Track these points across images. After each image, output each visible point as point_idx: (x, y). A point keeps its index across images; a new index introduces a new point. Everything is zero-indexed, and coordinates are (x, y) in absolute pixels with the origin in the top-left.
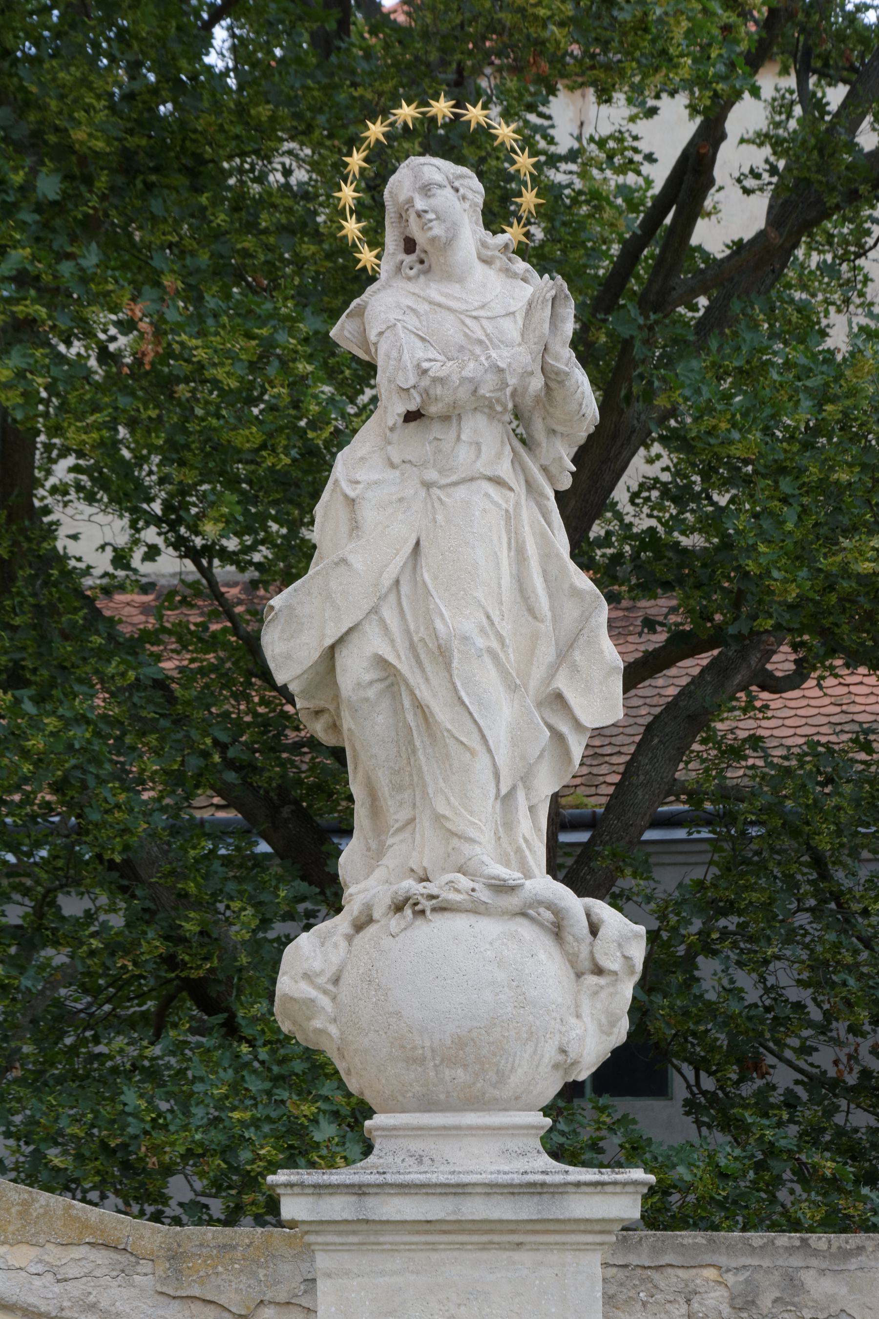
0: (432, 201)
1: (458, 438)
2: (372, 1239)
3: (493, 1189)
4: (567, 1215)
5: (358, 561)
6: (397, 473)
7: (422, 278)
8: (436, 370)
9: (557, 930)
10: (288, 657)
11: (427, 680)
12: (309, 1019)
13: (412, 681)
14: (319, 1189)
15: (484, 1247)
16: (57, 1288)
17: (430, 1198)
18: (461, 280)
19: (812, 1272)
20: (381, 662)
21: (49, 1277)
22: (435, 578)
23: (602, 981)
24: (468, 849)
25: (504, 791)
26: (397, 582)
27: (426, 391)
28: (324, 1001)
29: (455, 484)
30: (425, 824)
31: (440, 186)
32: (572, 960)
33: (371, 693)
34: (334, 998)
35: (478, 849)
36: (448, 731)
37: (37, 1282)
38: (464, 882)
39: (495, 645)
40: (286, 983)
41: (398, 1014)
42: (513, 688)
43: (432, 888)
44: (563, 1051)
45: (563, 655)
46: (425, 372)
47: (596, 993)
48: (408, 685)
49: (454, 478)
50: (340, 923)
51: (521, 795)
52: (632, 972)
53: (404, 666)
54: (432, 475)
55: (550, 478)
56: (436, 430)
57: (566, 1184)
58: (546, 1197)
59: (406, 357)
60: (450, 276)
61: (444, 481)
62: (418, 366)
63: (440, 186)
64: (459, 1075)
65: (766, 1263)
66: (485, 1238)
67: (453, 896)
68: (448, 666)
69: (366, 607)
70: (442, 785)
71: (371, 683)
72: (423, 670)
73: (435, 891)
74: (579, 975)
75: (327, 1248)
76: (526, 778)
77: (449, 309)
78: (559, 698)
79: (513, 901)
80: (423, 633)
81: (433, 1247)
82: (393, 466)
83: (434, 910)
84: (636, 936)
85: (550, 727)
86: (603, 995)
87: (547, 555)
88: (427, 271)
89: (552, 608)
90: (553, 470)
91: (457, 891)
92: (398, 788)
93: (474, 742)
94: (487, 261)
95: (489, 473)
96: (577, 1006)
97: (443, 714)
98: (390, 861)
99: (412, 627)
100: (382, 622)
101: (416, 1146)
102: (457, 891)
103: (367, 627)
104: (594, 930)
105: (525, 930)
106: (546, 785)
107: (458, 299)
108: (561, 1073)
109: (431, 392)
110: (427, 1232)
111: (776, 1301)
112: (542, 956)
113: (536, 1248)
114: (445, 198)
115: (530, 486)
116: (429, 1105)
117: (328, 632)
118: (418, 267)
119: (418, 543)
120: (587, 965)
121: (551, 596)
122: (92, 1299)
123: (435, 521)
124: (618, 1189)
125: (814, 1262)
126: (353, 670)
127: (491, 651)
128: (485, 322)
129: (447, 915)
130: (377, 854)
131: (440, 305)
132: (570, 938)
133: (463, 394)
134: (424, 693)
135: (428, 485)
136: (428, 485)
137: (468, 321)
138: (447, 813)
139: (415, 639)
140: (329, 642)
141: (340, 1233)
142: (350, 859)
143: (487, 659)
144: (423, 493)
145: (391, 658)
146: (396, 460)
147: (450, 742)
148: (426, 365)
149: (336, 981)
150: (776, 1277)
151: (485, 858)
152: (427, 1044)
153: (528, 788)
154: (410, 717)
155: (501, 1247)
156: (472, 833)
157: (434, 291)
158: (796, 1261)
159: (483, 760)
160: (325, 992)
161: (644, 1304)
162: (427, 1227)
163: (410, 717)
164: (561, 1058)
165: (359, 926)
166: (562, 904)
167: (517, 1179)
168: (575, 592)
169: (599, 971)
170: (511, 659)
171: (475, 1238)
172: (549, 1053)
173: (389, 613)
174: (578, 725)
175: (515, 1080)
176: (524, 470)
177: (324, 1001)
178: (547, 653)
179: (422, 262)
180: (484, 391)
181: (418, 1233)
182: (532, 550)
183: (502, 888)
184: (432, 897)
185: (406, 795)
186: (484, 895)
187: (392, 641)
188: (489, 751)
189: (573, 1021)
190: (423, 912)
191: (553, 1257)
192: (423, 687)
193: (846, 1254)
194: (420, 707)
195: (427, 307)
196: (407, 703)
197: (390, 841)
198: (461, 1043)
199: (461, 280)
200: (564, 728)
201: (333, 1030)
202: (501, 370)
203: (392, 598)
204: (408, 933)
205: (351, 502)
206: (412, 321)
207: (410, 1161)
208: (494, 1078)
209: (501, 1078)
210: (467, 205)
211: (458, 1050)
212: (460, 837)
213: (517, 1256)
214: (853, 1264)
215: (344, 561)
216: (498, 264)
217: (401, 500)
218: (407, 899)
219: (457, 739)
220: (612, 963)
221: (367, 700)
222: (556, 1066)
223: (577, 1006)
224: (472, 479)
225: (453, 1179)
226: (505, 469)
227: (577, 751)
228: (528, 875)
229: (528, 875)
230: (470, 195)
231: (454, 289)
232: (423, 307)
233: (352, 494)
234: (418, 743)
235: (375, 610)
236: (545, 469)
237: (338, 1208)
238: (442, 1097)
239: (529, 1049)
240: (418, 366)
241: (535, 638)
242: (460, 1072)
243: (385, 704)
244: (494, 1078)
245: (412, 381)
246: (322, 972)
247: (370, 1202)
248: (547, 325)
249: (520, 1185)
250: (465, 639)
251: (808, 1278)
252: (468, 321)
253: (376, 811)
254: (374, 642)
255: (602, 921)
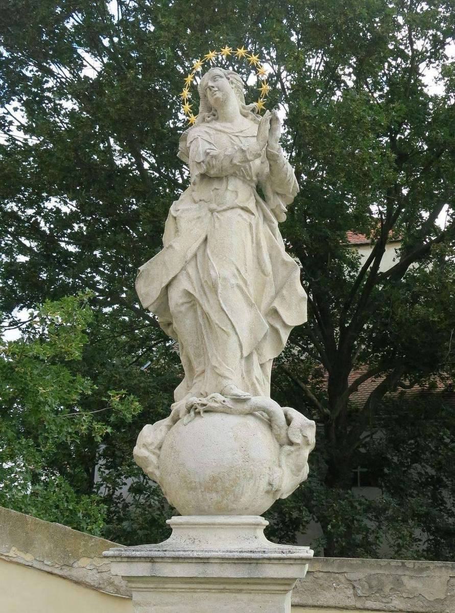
0: (216, 83)
1: (227, 188)
2: (161, 586)
3: (224, 560)
4: (264, 575)
5: (177, 246)
6: (198, 205)
7: (214, 121)
8: (213, 153)
9: (270, 423)
10: (147, 294)
11: (209, 301)
12: (147, 467)
13: (201, 302)
14: (131, 559)
15: (222, 591)
16: (98, 575)
17: (190, 565)
18: (231, 121)
19: (407, 577)
20: (188, 294)
21: (95, 571)
22: (212, 252)
23: (292, 448)
24: (225, 382)
25: (245, 354)
26: (195, 255)
27: (209, 163)
28: (153, 458)
29: (225, 210)
30: (208, 374)
31: (221, 77)
32: (277, 438)
33: (183, 309)
34: (159, 457)
35: (230, 382)
36: (217, 324)
37: (90, 573)
38: (220, 398)
39: (241, 283)
40: (138, 451)
41: (183, 464)
42: (251, 305)
43: (204, 401)
44: (270, 484)
45: (277, 293)
46: (208, 154)
47: (289, 455)
48: (200, 305)
49: (225, 207)
50: (167, 421)
51: (255, 357)
52: (308, 444)
53: (197, 295)
54: (214, 206)
55: (276, 216)
56: (216, 185)
57: (264, 558)
58: (253, 565)
59: (200, 149)
60: (227, 119)
61: (219, 209)
62: (206, 151)
63: (221, 77)
64: (218, 497)
65: (387, 573)
66: (222, 587)
68: (216, 292)
69: (180, 268)
70: (215, 352)
71: (183, 304)
72: (205, 294)
74: (281, 445)
75: (139, 590)
76: (257, 348)
77: (224, 132)
78: (275, 312)
79: (246, 407)
81: (194, 591)
82: (195, 202)
83: (206, 412)
84: (310, 425)
85: (271, 326)
86: (293, 455)
87: (272, 247)
88: (217, 119)
89: (273, 270)
90: (277, 212)
91: (216, 402)
92: (198, 356)
94: (245, 116)
95: (241, 205)
96: (279, 461)
97: (215, 317)
98: (194, 390)
99: (202, 276)
100: (188, 274)
101: (192, 533)
102: (216, 402)
103: (180, 277)
104: (289, 422)
105: (251, 422)
106: (270, 353)
107: (228, 128)
108: (271, 496)
109: (211, 163)
110: (190, 583)
111: (392, 589)
112: (260, 435)
113: (249, 592)
114: (224, 82)
115: (266, 218)
116: (201, 512)
117: (164, 281)
118: (212, 117)
119: (206, 239)
120: (285, 440)
121: (273, 266)
122: (112, 580)
123: (214, 227)
124: (292, 562)
125: (407, 573)
126: (176, 297)
127: (239, 286)
128: (241, 138)
129: (212, 414)
130: (189, 388)
131: (220, 131)
132: (276, 427)
133: (226, 163)
134: (207, 308)
135: (212, 211)
136: (212, 211)
137: (233, 137)
138: (217, 365)
139: (203, 282)
140: (164, 285)
141: (143, 582)
142: (178, 391)
143: (236, 289)
144: (210, 215)
146: (197, 199)
148: (208, 151)
149: (160, 448)
150: (391, 578)
151: (233, 386)
152: (197, 480)
153: (260, 355)
154: (201, 320)
155: (231, 591)
156: (227, 374)
157: (218, 125)
158: (400, 572)
159: (234, 338)
160: (154, 453)
161: (335, 589)
162: (191, 580)
163: (201, 320)
164: (270, 487)
165: (175, 421)
166: (271, 409)
167: (237, 555)
168: (285, 263)
169: (291, 443)
170: (252, 291)
171: (216, 586)
172: (263, 485)
173: (191, 270)
174: (285, 325)
175: (245, 500)
176: (262, 210)
177: (153, 458)
178: (270, 290)
179: (214, 115)
180: (235, 161)
181: (186, 583)
182: (264, 244)
183: (238, 400)
184: (205, 405)
185: (202, 359)
186: (229, 403)
187: (192, 283)
188: (237, 334)
189: (277, 469)
190: (199, 413)
191: (258, 597)
193: (421, 570)
194: (206, 316)
195: (214, 132)
196: (199, 313)
198: (214, 480)
199: (231, 121)
200: (278, 326)
201: (157, 473)
202: (243, 151)
203: (193, 263)
204: (191, 424)
205: (175, 218)
206: (206, 137)
207: (188, 542)
208: (233, 499)
209: (237, 499)
210: (233, 86)
211: (213, 484)
212: (222, 377)
213: (239, 596)
214: (425, 574)
216: (250, 117)
217: (199, 218)
218: (192, 406)
219: (220, 328)
220: (298, 439)
221: (181, 312)
222: (268, 492)
223: (279, 461)
224: (233, 208)
225: (202, 555)
226: (251, 205)
227: (285, 336)
228: (256, 393)
229: (256, 393)
230: (235, 81)
231: (228, 125)
232: (212, 132)
233: (175, 215)
234: (204, 332)
235: (184, 268)
236: (273, 211)
237: (140, 570)
238: (206, 508)
239: (252, 482)
240: (206, 151)
241: (264, 285)
242: (214, 495)
243: (191, 314)
244: (233, 499)
245: (202, 159)
246: (152, 444)
247: (157, 566)
248: (267, 132)
249: (237, 559)
250: (225, 279)
251: (405, 580)
252: (233, 137)
253: (191, 369)
254: (184, 284)
255: (292, 418)
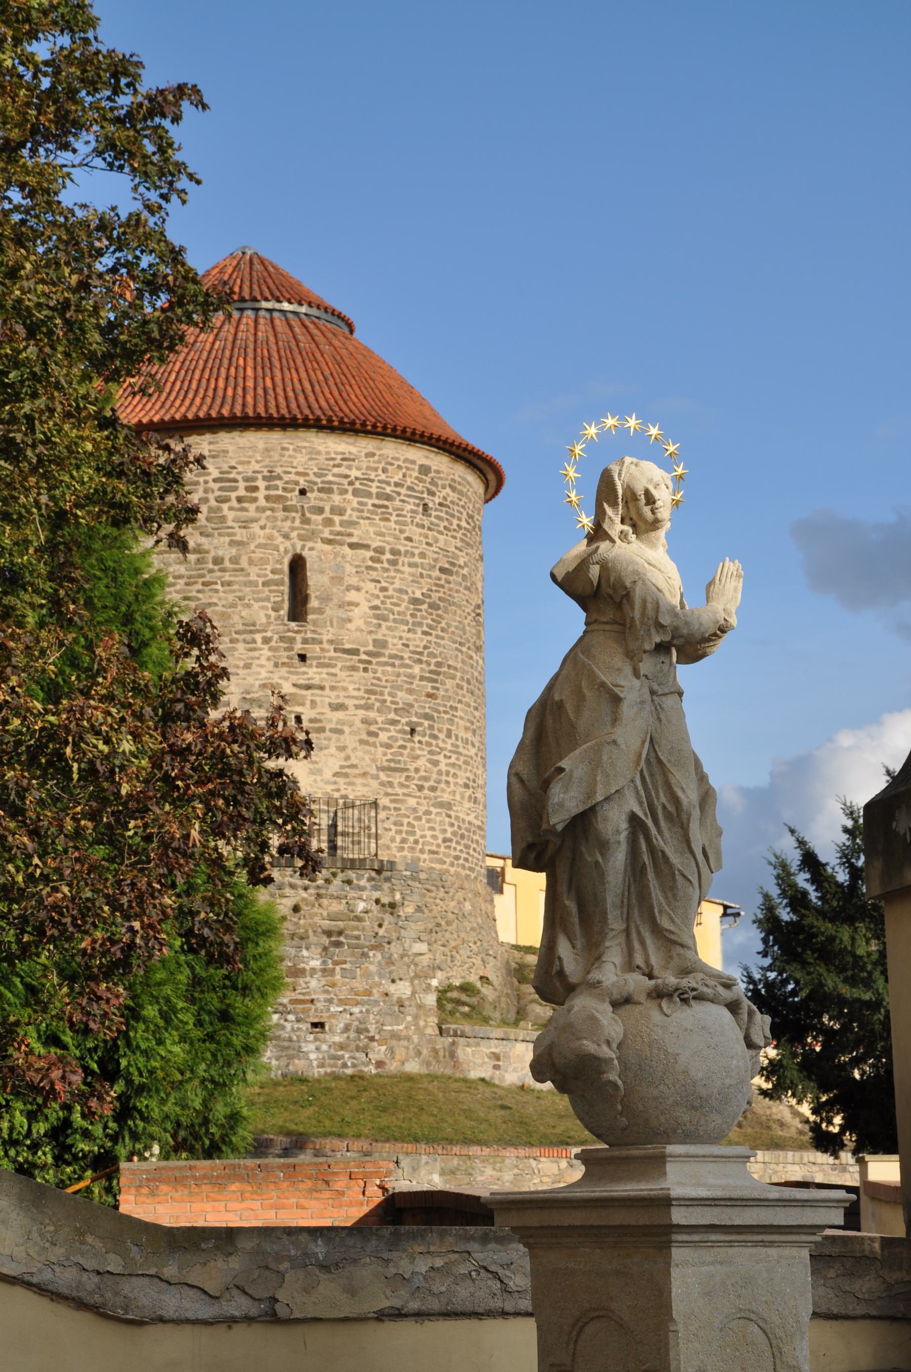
10: (561, 805)
20: (633, 819)
36: (679, 871)
54: (656, 687)
67: (705, 989)
73: (694, 985)
80: (663, 799)
83: (694, 998)
91: (707, 986)
93: (696, 883)
102: (707, 986)
123: (659, 720)
134: (658, 841)
138: (672, 928)
145: (641, 814)
147: (679, 878)
184: (694, 989)
192: (659, 837)
197: (607, 944)
212: (682, 946)
215: (614, 742)
218: (676, 990)
